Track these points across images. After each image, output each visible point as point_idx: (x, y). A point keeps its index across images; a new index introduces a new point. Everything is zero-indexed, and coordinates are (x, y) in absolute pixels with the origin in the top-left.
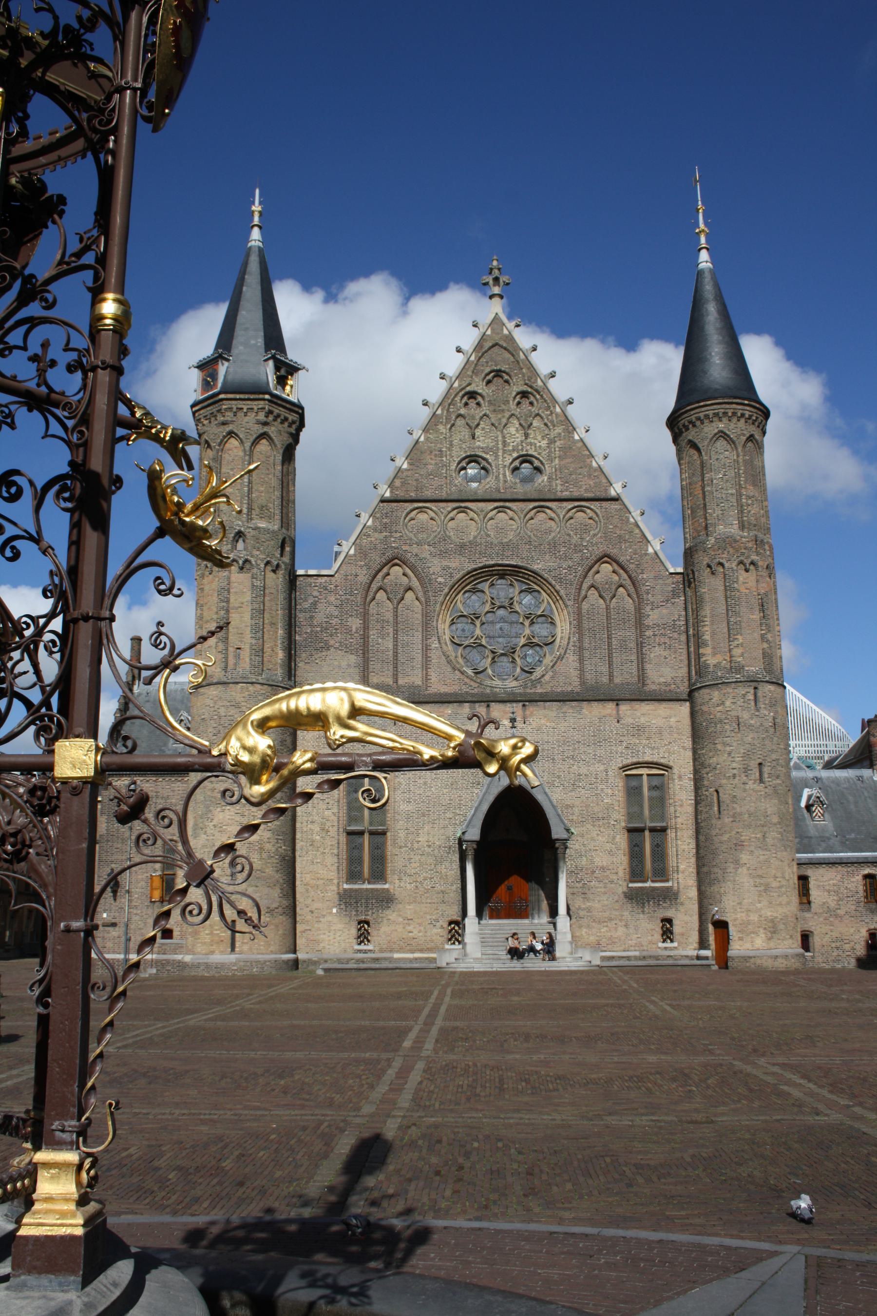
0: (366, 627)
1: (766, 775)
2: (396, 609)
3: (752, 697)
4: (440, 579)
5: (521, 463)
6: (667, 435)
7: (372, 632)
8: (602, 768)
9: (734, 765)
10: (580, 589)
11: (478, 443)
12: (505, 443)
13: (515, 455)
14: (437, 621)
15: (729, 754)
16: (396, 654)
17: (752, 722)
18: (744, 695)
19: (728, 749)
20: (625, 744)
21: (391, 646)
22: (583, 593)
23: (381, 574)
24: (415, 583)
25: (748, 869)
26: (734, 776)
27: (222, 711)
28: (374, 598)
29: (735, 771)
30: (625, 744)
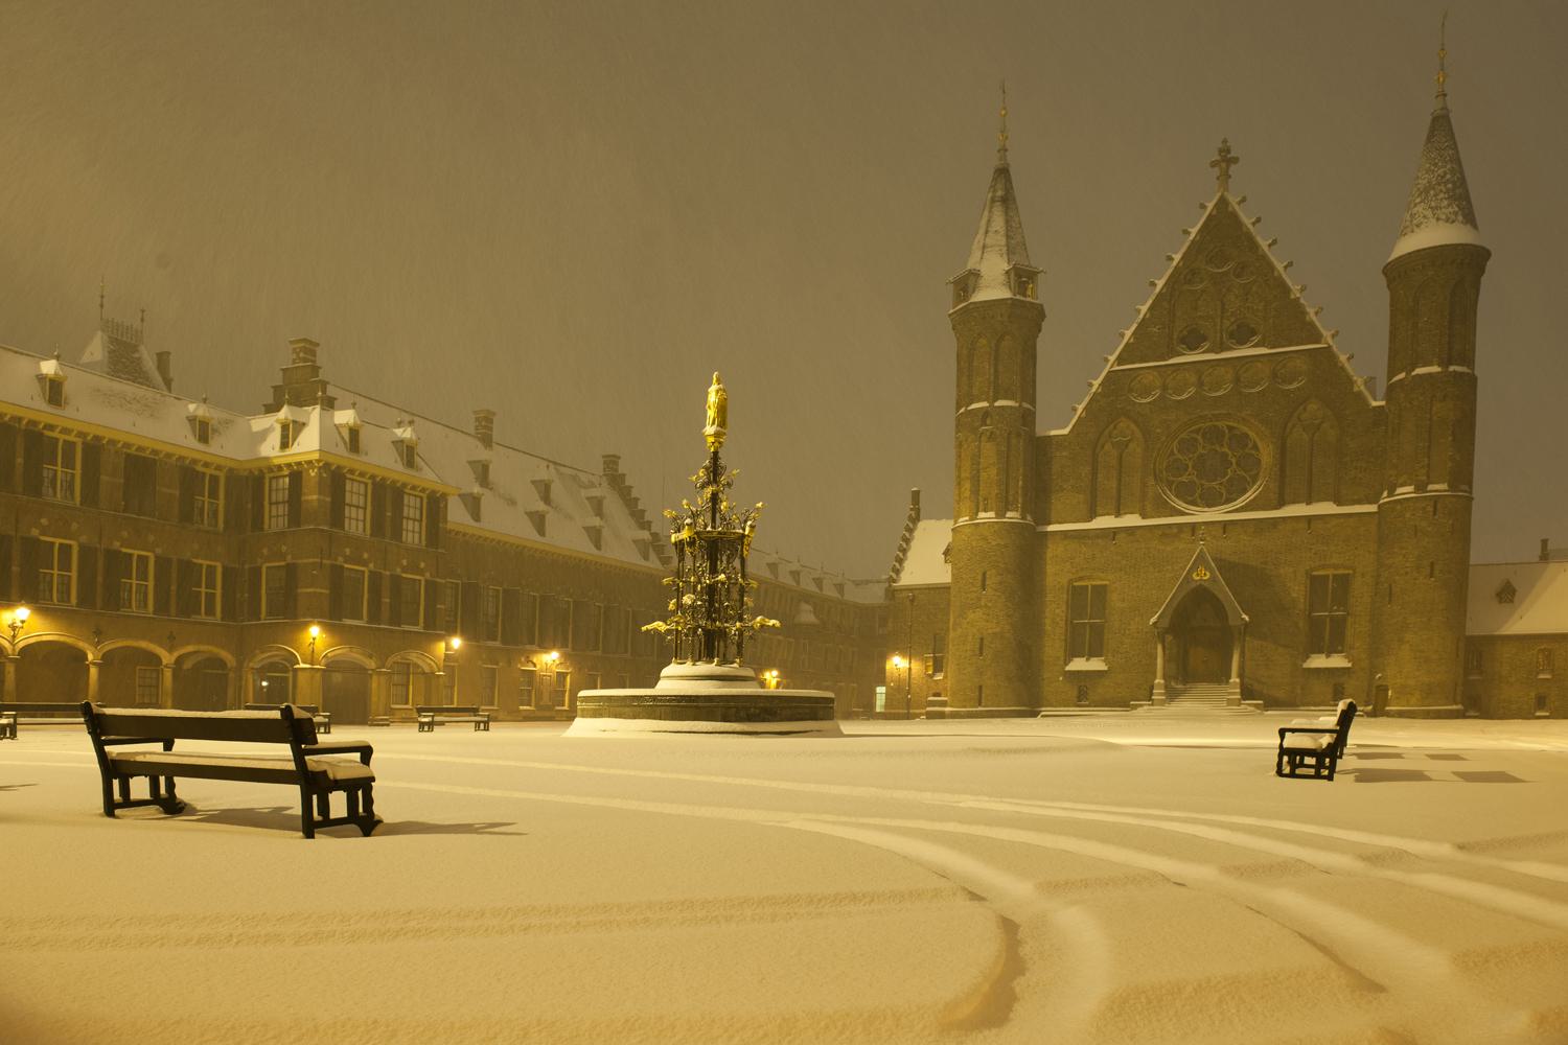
0: (1094, 473)
1: (1436, 572)
2: (1120, 458)
3: (1432, 509)
4: (1158, 430)
5: (1238, 326)
6: (1383, 281)
7: (1100, 477)
8: (1291, 570)
9: (1408, 565)
10: (1285, 427)
11: (1199, 314)
12: (1223, 310)
13: (1233, 320)
14: (1155, 464)
15: (1404, 556)
16: (1119, 491)
17: (1429, 529)
18: (1424, 508)
19: (1404, 552)
20: (1313, 551)
21: (1114, 486)
22: (1288, 430)
23: (1107, 432)
24: (1138, 434)
25: (1411, 645)
26: (1407, 573)
27: (974, 544)
28: (1103, 447)
29: (1408, 570)
30: (1313, 551)
